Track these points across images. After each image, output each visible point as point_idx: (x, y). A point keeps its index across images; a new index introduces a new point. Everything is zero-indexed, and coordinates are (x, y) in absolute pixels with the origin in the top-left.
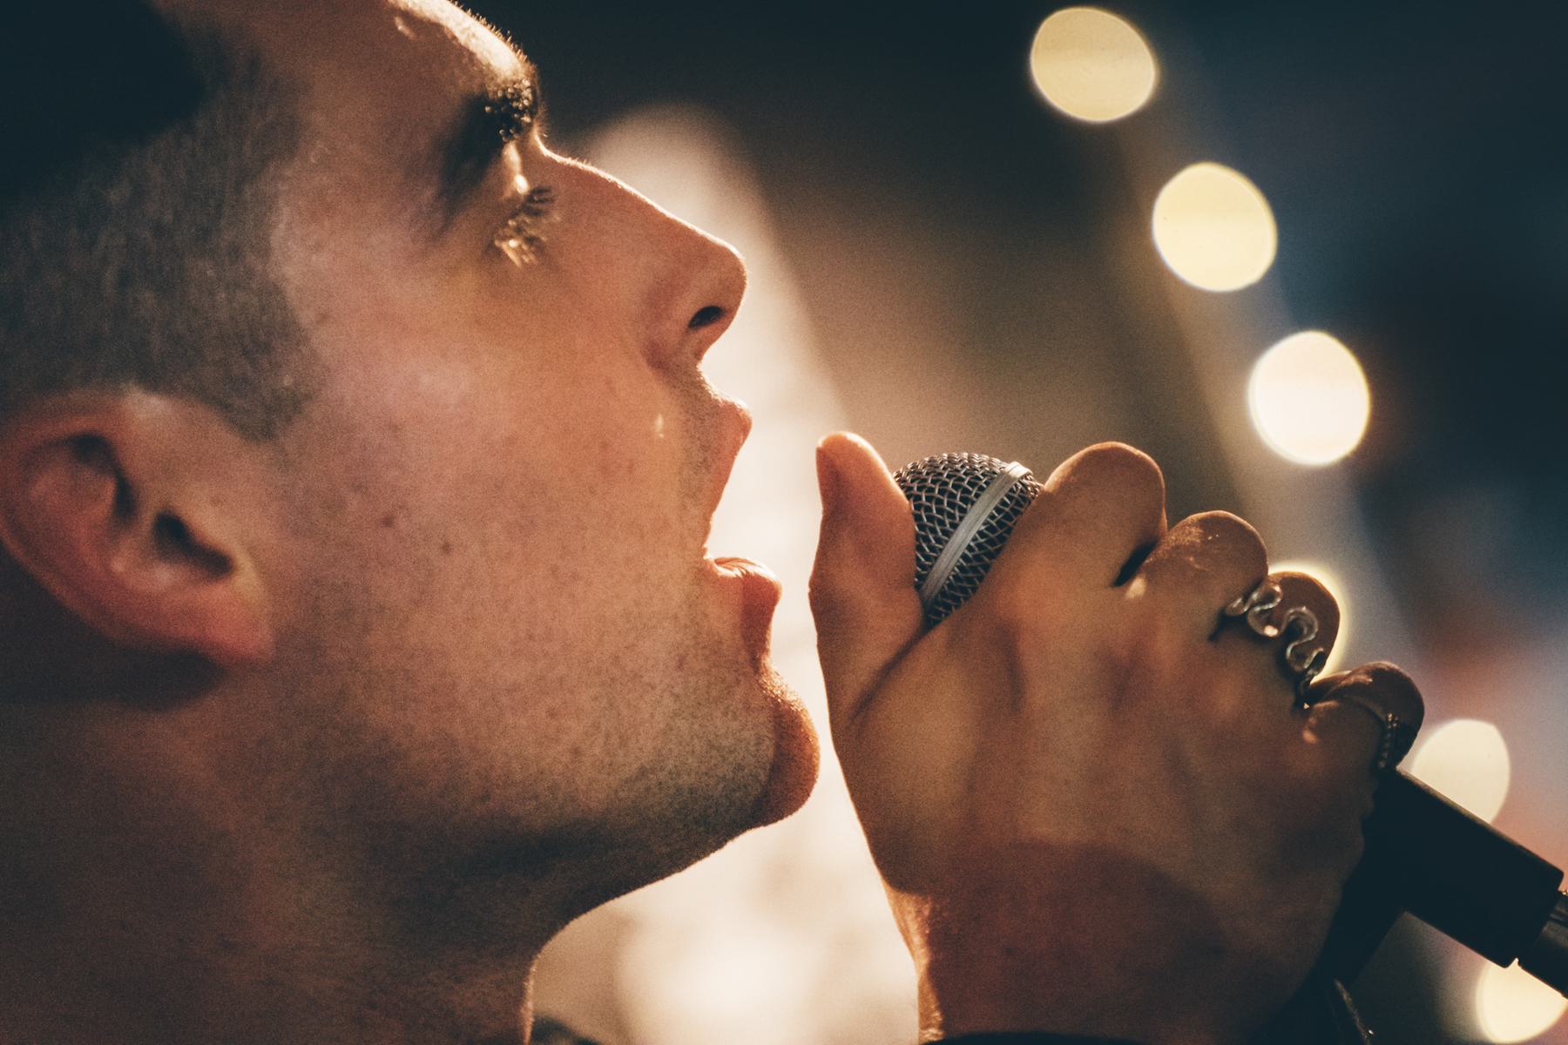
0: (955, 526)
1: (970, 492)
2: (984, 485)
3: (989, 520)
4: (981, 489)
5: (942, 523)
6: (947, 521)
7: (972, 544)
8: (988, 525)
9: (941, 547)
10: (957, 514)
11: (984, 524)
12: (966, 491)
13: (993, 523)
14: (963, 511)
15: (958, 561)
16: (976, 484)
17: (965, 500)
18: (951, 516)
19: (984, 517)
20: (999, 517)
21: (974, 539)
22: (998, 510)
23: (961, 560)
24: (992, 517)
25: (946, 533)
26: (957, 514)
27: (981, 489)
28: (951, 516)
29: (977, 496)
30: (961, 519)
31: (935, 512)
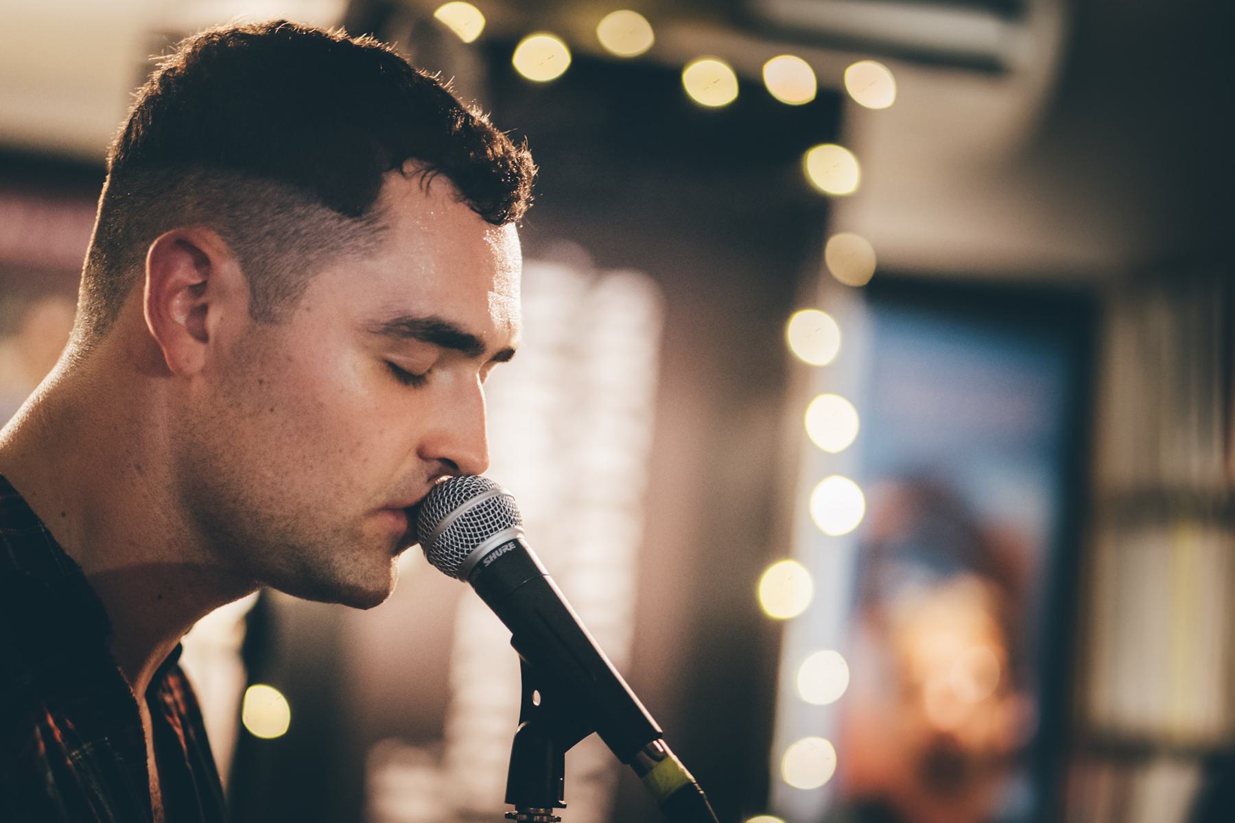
0: (456, 508)
5: (451, 505)
6: (454, 505)
7: (460, 518)
11: (469, 511)
12: (469, 495)
14: (462, 502)
17: (465, 498)
18: (456, 503)
19: (470, 508)
22: (478, 507)
25: (452, 510)
26: (459, 503)
27: (475, 495)
28: (456, 503)
29: (472, 497)
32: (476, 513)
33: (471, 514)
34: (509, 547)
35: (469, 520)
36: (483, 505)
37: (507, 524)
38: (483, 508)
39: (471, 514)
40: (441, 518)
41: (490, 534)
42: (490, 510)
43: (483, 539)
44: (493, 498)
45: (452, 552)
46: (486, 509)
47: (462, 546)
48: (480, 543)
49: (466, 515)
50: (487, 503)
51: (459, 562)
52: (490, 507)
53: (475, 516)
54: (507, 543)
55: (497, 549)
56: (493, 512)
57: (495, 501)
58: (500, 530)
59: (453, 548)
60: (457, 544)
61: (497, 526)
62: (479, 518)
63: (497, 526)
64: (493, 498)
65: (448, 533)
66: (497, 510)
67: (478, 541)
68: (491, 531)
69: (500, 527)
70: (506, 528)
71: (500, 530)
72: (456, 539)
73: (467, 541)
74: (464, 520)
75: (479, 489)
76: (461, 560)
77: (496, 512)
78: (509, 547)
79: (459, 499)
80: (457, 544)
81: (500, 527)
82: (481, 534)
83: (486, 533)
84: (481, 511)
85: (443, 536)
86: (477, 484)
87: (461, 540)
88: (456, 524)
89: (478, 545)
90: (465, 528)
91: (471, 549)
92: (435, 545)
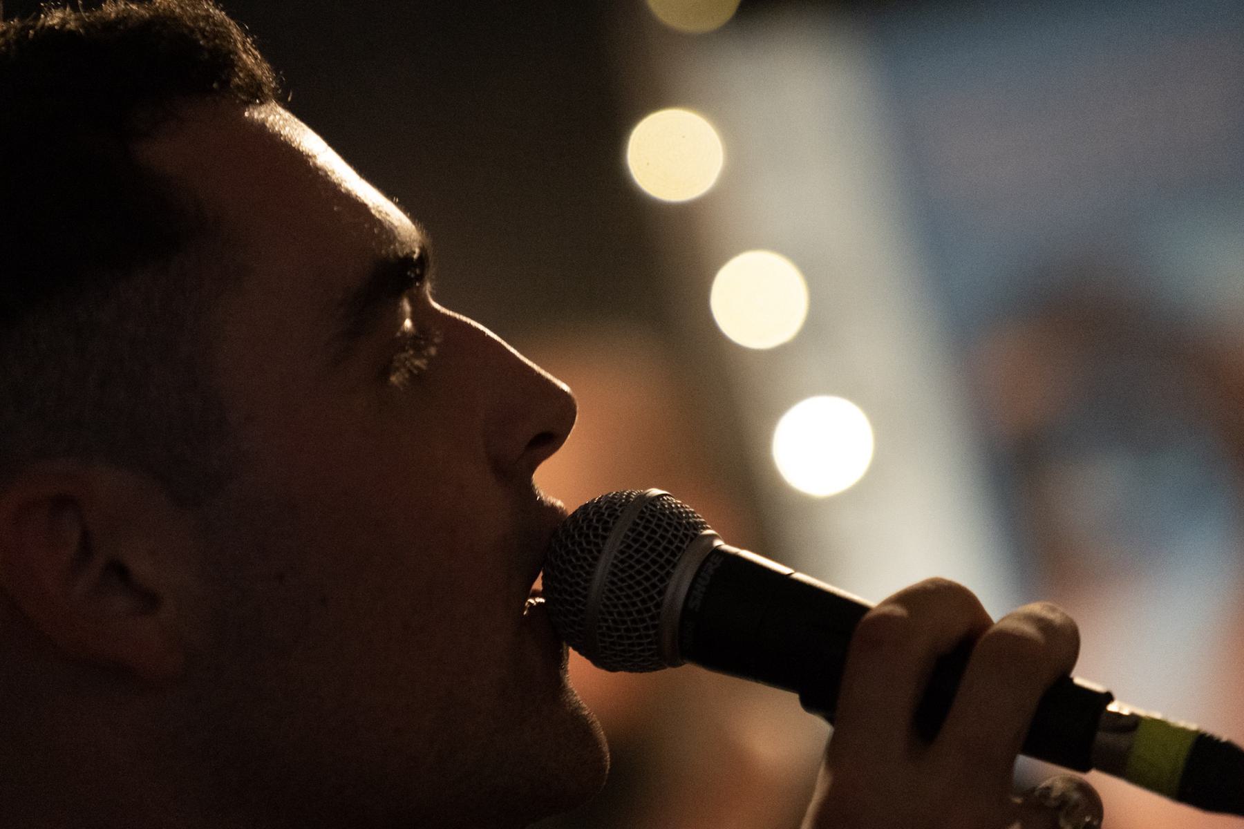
0: (599, 551)
1: (608, 522)
2: (619, 514)
3: (625, 540)
4: (617, 517)
5: (590, 552)
7: (615, 562)
8: (624, 545)
9: (593, 570)
10: (600, 542)
11: (621, 545)
13: (629, 541)
14: (604, 538)
15: (607, 578)
16: (613, 514)
17: (605, 530)
18: (597, 544)
20: (632, 535)
21: (616, 557)
22: (633, 531)
23: (609, 576)
24: (627, 536)
25: (596, 559)
26: (600, 542)
27: (617, 517)
29: (614, 523)
30: (604, 544)
31: (592, 537)
32: (635, 541)
33: (629, 547)
34: (714, 564)
35: (631, 557)
36: (638, 524)
37: (690, 533)
38: (640, 528)
39: (629, 547)
40: (585, 589)
41: (675, 560)
42: (653, 526)
43: (669, 574)
44: (646, 507)
45: (634, 621)
46: (646, 528)
47: (643, 601)
48: (668, 581)
49: (622, 552)
50: (641, 518)
51: (652, 632)
52: (650, 522)
53: (636, 546)
54: (703, 564)
55: (697, 576)
56: (659, 526)
57: (651, 510)
58: (685, 546)
59: (630, 614)
60: (634, 604)
61: (677, 543)
62: (644, 545)
63: (677, 543)
64: (646, 507)
65: (611, 596)
66: (662, 521)
67: (662, 580)
68: (674, 555)
69: (682, 542)
70: (692, 539)
71: (685, 546)
72: (628, 596)
73: (646, 590)
74: (622, 561)
75: (617, 507)
76: (655, 627)
77: (664, 524)
78: (714, 564)
79: (596, 536)
80: (634, 604)
81: (682, 542)
82: (662, 567)
83: (668, 561)
84: (641, 534)
85: (605, 605)
86: (610, 502)
87: (637, 594)
88: (614, 575)
89: (666, 587)
90: (632, 562)
91: (658, 599)
92: (600, 627)
